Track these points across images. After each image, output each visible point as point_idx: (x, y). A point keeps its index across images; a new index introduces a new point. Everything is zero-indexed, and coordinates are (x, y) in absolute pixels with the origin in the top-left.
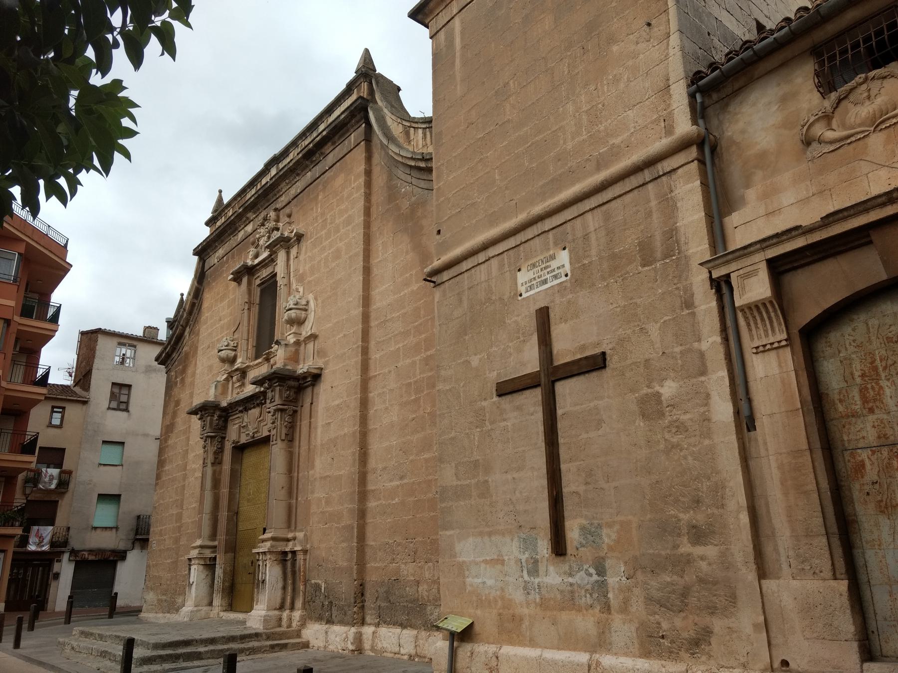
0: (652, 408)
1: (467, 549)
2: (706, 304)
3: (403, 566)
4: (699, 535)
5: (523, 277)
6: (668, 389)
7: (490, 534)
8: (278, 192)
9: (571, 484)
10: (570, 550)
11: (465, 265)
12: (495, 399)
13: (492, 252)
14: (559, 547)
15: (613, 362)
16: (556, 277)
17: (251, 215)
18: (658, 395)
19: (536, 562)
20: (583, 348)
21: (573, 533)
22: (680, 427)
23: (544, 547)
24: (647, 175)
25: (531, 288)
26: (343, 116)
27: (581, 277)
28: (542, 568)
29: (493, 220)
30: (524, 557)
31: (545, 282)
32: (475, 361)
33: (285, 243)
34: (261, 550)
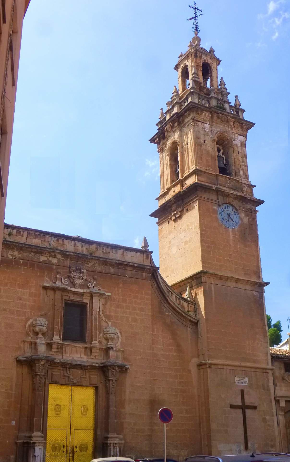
0: (264, 420)
1: (221, 447)
2: (274, 403)
3: (171, 451)
4: (272, 446)
5: (236, 379)
6: (268, 417)
7: (228, 443)
8: (88, 262)
9: (249, 434)
10: (249, 448)
11: (219, 367)
12: (229, 408)
13: (228, 367)
14: (246, 448)
15: (258, 408)
16: (245, 383)
17: (59, 256)
18: (266, 418)
19: (241, 451)
20: (251, 403)
21: (249, 445)
22: (269, 425)
23: (243, 447)
24: (265, 371)
25: (239, 383)
26: (148, 267)
27: (250, 386)
28: (242, 452)
29: (227, 358)
30: (238, 449)
31: (242, 383)
32: (223, 396)
33: (101, 295)
34: (115, 442)
